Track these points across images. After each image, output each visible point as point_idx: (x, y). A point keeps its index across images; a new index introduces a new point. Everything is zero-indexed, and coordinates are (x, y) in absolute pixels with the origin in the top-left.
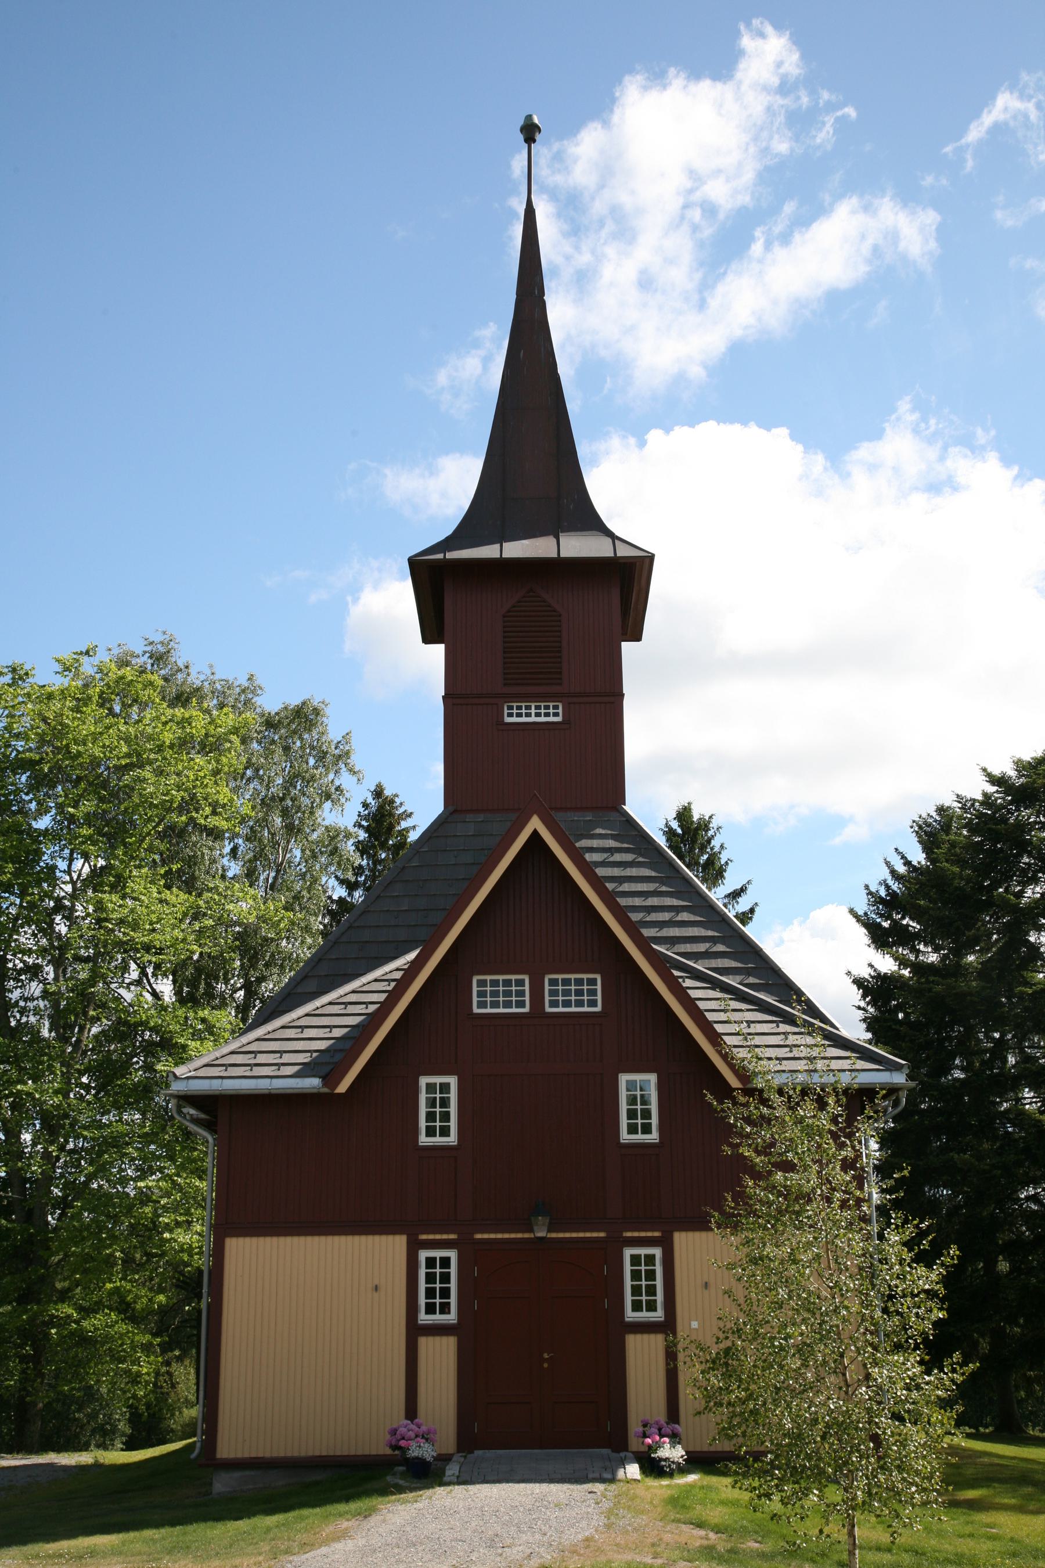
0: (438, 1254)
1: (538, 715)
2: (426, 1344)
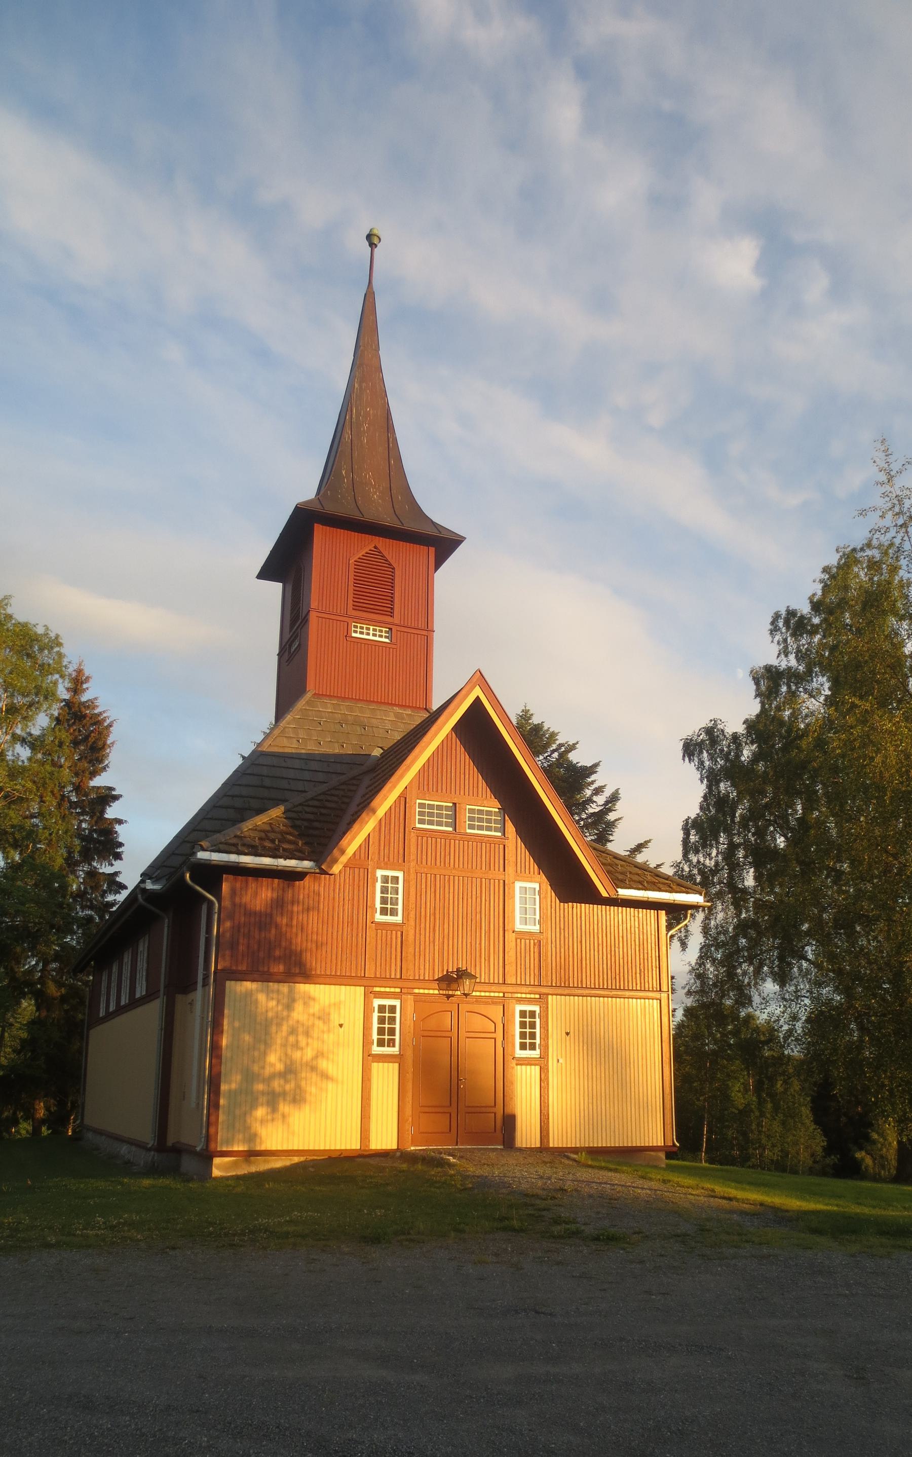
0: (387, 1002)
1: (374, 635)
2: (377, 1069)
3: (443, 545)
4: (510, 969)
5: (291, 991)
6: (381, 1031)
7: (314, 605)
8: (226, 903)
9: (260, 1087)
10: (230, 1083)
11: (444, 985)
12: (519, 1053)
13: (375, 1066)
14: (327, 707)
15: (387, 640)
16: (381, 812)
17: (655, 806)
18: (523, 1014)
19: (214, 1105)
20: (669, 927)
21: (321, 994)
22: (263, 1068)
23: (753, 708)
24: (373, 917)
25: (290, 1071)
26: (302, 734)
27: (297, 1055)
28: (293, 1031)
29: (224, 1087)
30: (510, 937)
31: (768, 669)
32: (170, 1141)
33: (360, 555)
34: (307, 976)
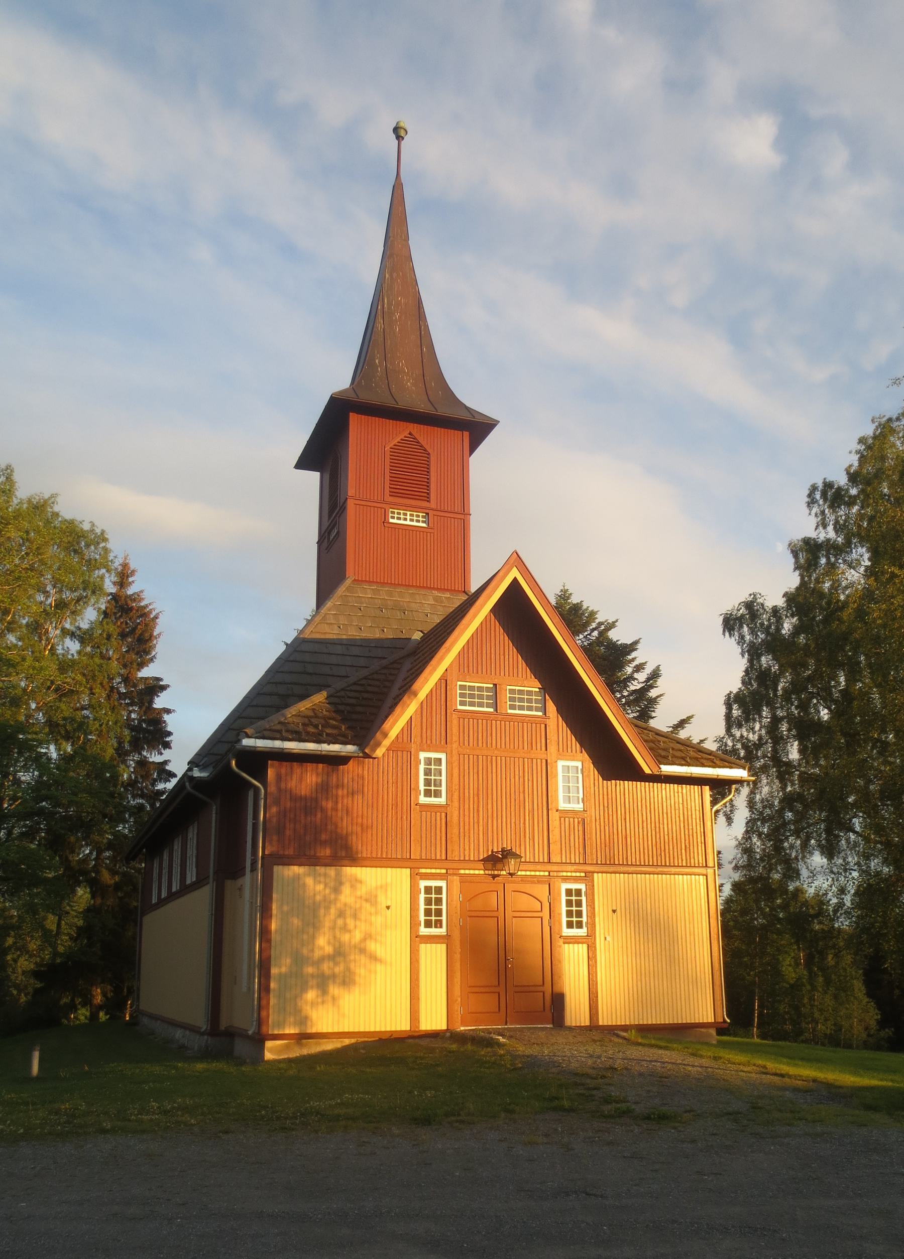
0: (433, 883)
1: (412, 520)
3: (477, 429)
4: (554, 848)
5: (338, 875)
6: (428, 912)
7: (351, 492)
8: (272, 788)
9: (310, 970)
10: (280, 967)
11: (490, 866)
12: (566, 932)
13: (423, 947)
14: (366, 593)
15: (424, 525)
16: (422, 695)
17: (697, 683)
18: (569, 892)
19: (265, 988)
20: (714, 802)
21: (368, 877)
22: (313, 951)
23: (793, 581)
24: (417, 798)
25: (339, 953)
26: (343, 620)
27: (346, 937)
29: (274, 971)
30: (555, 816)
31: (807, 541)
32: (223, 1025)
33: (395, 442)
34: (353, 859)
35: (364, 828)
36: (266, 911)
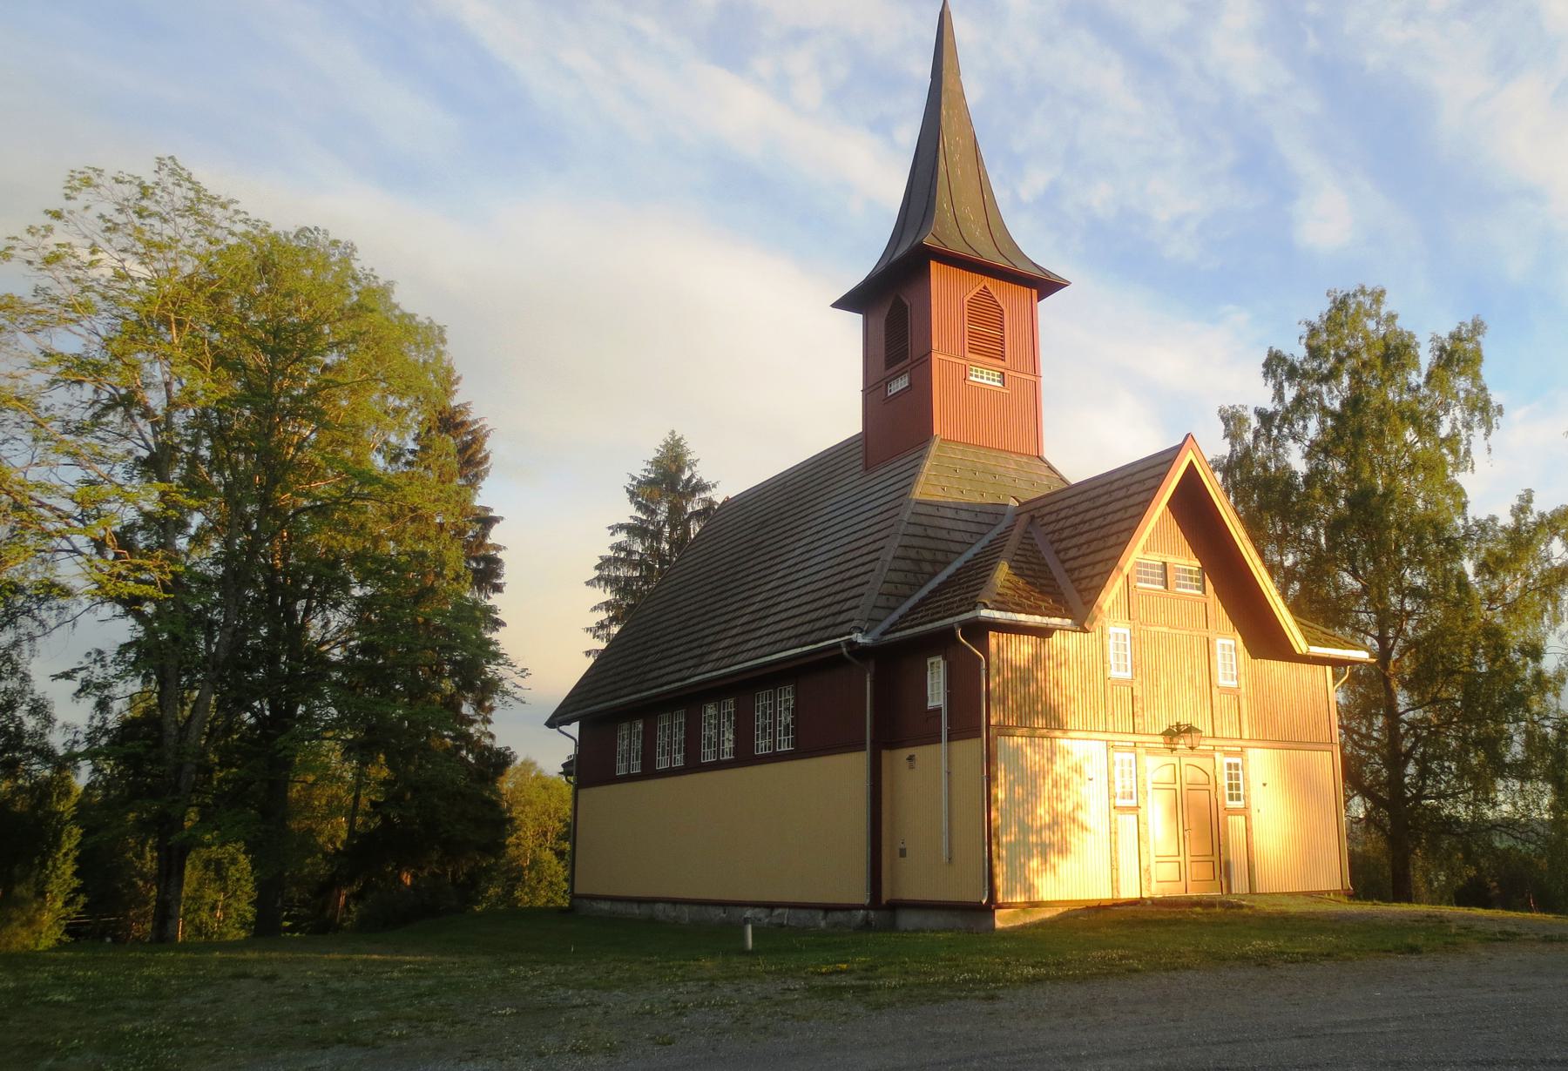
3: (1045, 285)
7: (935, 346)
8: (993, 659)
18: (1229, 766)
25: (1055, 823)
27: (1060, 807)
28: (1055, 784)
35: (1070, 699)
36: (991, 779)
